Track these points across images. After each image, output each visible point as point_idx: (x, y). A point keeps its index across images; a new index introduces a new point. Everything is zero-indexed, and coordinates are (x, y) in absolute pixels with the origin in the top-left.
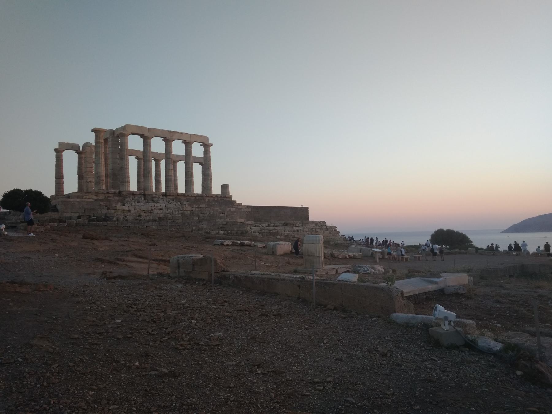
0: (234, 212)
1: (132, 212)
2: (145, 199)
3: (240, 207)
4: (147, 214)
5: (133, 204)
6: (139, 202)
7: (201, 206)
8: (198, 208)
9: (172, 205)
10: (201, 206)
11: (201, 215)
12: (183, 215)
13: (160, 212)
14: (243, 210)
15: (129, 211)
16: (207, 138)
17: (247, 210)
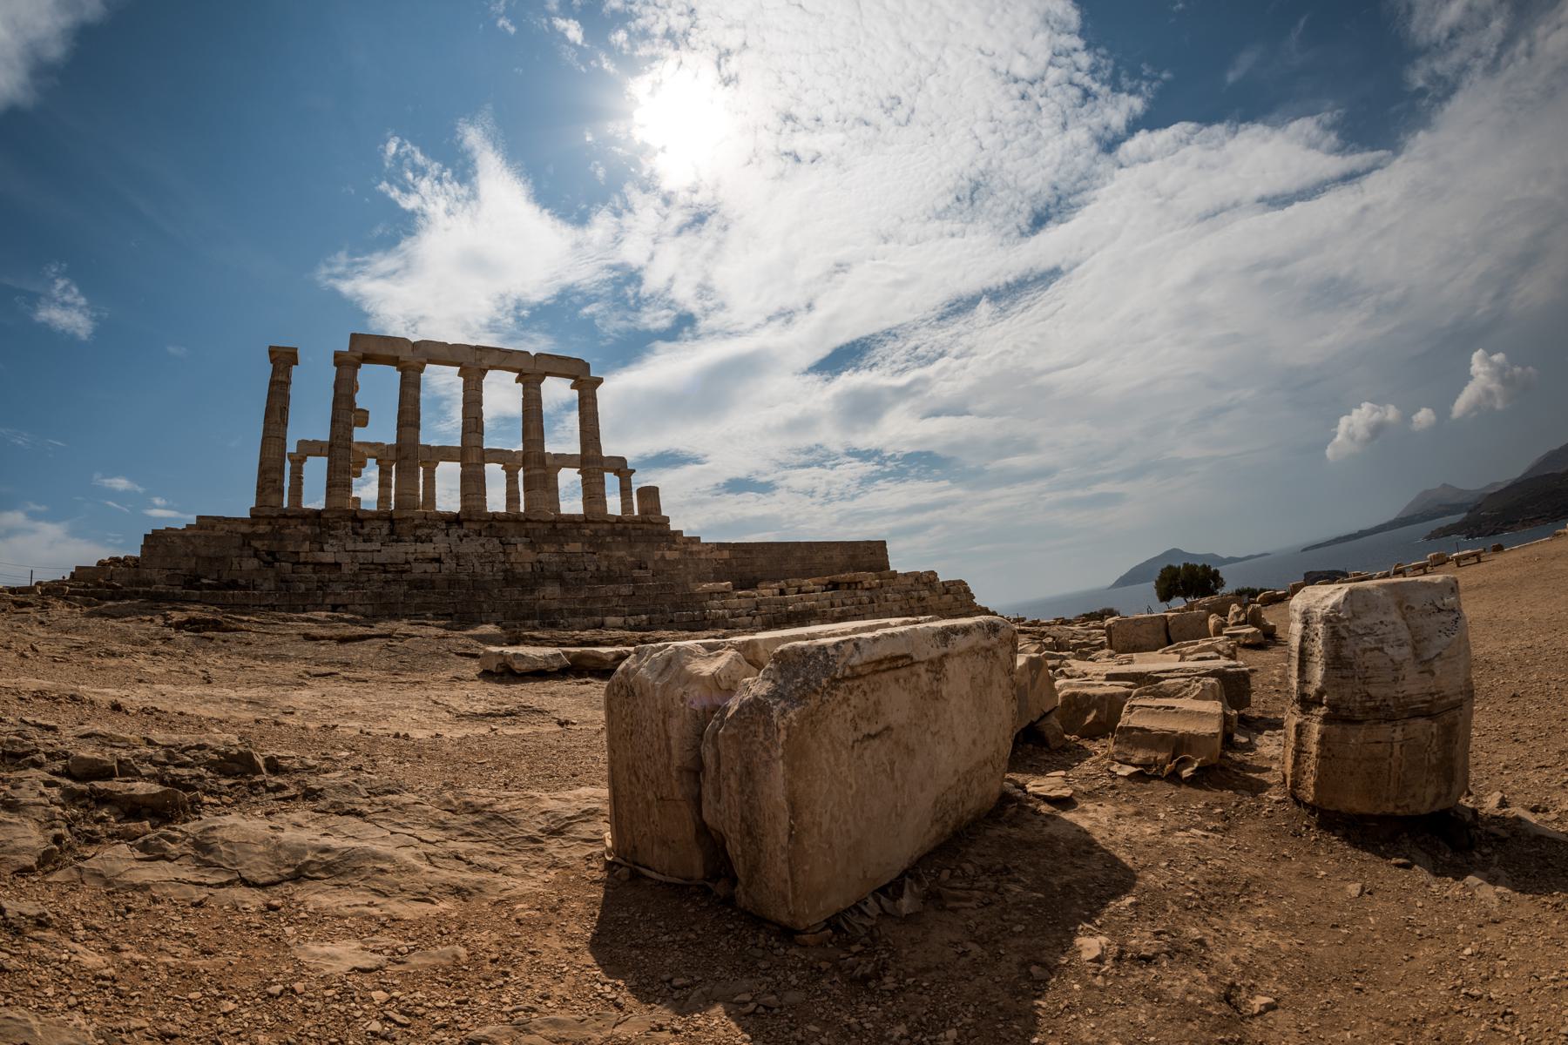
0: (678, 562)
1: (345, 569)
2: (392, 532)
3: (695, 548)
4: (390, 576)
5: (350, 546)
6: (368, 539)
7: (567, 548)
8: (559, 553)
9: (470, 547)
10: (567, 548)
11: (569, 576)
12: (510, 578)
13: (431, 568)
14: (703, 556)
15: (337, 565)
16: (587, 366)
17: (716, 555)
